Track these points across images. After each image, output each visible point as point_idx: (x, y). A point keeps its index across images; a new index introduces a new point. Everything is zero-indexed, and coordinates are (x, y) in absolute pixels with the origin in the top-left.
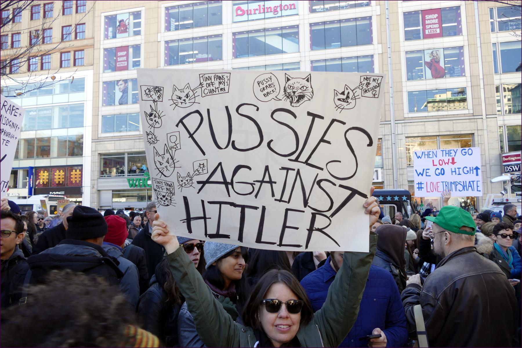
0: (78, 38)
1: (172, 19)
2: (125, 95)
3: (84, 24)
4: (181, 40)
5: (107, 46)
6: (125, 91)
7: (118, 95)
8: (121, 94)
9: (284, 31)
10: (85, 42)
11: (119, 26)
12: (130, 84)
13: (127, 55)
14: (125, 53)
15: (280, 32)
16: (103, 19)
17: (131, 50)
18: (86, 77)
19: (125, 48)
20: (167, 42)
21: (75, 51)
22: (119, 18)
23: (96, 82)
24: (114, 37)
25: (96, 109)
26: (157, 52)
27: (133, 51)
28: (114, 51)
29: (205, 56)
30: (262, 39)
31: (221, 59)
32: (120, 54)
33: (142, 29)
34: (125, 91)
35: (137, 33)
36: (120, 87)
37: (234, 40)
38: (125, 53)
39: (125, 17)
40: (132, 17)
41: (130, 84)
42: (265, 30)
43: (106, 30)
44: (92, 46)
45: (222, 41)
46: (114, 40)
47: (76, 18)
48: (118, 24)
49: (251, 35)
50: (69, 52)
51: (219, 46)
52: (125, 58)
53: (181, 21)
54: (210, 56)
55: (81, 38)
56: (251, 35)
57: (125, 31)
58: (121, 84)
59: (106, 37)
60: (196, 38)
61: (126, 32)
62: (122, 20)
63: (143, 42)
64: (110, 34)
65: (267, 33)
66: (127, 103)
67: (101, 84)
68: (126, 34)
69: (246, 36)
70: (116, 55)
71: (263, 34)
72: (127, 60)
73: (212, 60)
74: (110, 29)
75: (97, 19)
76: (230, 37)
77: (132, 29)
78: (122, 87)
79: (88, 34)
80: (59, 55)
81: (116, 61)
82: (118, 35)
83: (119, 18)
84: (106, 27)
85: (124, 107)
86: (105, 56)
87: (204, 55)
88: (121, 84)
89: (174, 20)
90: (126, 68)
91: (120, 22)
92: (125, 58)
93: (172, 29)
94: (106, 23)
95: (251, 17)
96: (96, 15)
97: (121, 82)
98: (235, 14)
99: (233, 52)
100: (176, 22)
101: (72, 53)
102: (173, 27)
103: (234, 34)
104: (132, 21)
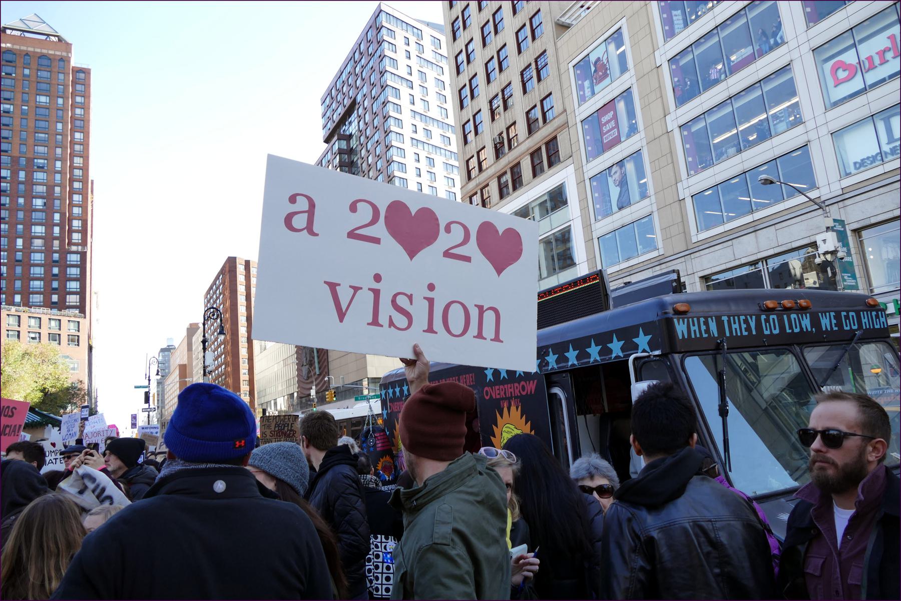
1: (674, 13)
2: (624, 189)
6: (623, 183)
7: (615, 192)
8: (618, 189)
11: (595, 71)
12: (630, 167)
13: (615, 117)
14: (612, 113)
16: (571, 70)
18: (566, 180)
19: (610, 105)
22: (593, 58)
23: (580, 182)
25: (587, 227)
32: (604, 119)
34: (623, 183)
36: (614, 177)
40: (612, 47)
41: (630, 167)
43: (581, 88)
44: (566, 125)
47: (539, 89)
48: (593, 69)
55: (551, 118)
57: (605, 75)
58: (616, 172)
61: (607, 76)
63: (634, 80)
64: (588, 92)
66: (629, 204)
67: (587, 182)
68: (607, 81)
70: (600, 125)
72: (617, 126)
74: (587, 84)
75: (564, 77)
78: (617, 176)
80: (529, 158)
81: (602, 134)
83: (593, 58)
84: (580, 82)
85: (625, 212)
88: (616, 172)
90: (617, 141)
92: (613, 123)
94: (577, 78)
96: (562, 71)
97: (615, 169)
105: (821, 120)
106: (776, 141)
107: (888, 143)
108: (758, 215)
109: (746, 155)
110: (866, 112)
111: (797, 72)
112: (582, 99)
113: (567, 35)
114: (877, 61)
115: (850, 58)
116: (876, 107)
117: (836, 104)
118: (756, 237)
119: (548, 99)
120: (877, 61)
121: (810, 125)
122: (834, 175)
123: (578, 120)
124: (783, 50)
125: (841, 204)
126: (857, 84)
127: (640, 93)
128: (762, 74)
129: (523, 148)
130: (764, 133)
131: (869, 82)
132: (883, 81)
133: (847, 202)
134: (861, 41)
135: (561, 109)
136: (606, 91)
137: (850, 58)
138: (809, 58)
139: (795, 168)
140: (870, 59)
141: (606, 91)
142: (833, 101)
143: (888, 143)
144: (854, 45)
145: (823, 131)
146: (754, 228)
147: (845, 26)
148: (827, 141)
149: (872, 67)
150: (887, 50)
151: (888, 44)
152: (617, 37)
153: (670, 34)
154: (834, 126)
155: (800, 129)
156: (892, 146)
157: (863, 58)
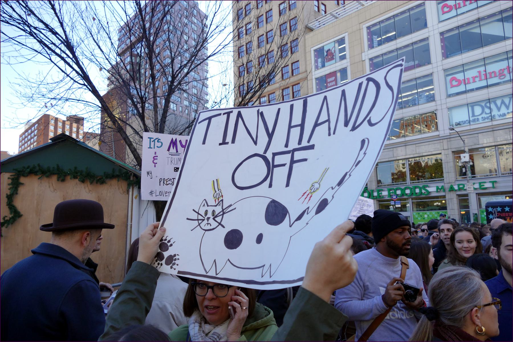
0: (294, 75)
1: (374, 37)
3: (298, 61)
4: (385, 54)
5: (318, 76)
9: (504, 15)
10: (300, 76)
11: (327, 55)
13: (336, 80)
15: (499, 17)
16: (312, 52)
17: (339, 75)
19: (334, 74)
20: (371, 59)
21: (293, 86)
22: (326, 49)
24: (323, 66)
26: (363, 70)
27: (341, 74)
28: (324, 79)
29: (411, 63)
30: (477, 31)
31: (429, 63)
32: (329, 80)
33: (347, 53)
35: (343, 58)
37: (442, 41)
38: (333, 78)
39: (330, 47)
40: (337, 45)
42: (479, 20)
43: (316, 61)
45: (428, 44)
46: (323, 69)
48: (325, 54)
49: (461, 30)
50: (289, 87)
51: (426, 50)
52: (334, 83)
53: (383, 36)
54: (417, 62)
56: (461, 30)
57: (332, 59)
59: (317, 68)
60: (400, 49)
61: (333, 59)
62: (329, 50)
63: (349, 64)
64: (320, 65)
65: (482, 23)
68: (334, 61)
69: (456, 32)
70: (326, 82)
71: (478, 24)
73: (419, 66)
75: (308, 55)
76: (438, 38)
77: (338, 55)
79: (302, 69)
80: (281, 91)
82: (326, 64)
83: (326, 49)
86: (317, 84)
87: (410, 63)
89: (376, 37)
91: (327, 51)
93: (375, 46)
94: (316, 56)
95: (460, 11)
98: (441, 12)
99: (443, 53)
100: (378, 38)
101: (291, 88)
102: (375, 43)
103: (442, 34)
104: (338, 47)
105: (444, 101)
106: (420, 107)
107: (472, 117)
108: (407, 139)
109: (404, 110)
110: (465, 102)
111: (435, 78)
112: (317, 68)
113: (311, 34)
114: (471, 80)
115: (460, 76)
116: (470, 101)
117: (449, 96)
118: (406, 149)
119: (296, 63)
120: (471, 80)
121: (438, 102)
122: (447, 126)
123: (314, 77)
124: (429, 66)
125: (449, 140)
126: (462, 88)
127: (351, 72)
128: (418, 75)
129: (277, 85)
130: (414, 103)
131: (467, 89)
132: (472, 90)
133: (451, 139)
134: (467, 70)
135: (304, 70)
136: (331, 67)
137: (460, 76)
138: (442, 74)
139: (429, 120)
140: (468, 79)
141: (331, 67)
142: (449, 93)
143: (472, 117)
144: (463, 71)
145: (444, 106)
146: (405, 144)
147: (460, 63)
148: (445, 111)
149: (469, 83)
150: (477, 77)
151: (477, 74)
152: (341, 41)
153: (371, 46)
154: (450, 105)
155: (433, 104)
156: (473, 118)
157: (466, 78)
